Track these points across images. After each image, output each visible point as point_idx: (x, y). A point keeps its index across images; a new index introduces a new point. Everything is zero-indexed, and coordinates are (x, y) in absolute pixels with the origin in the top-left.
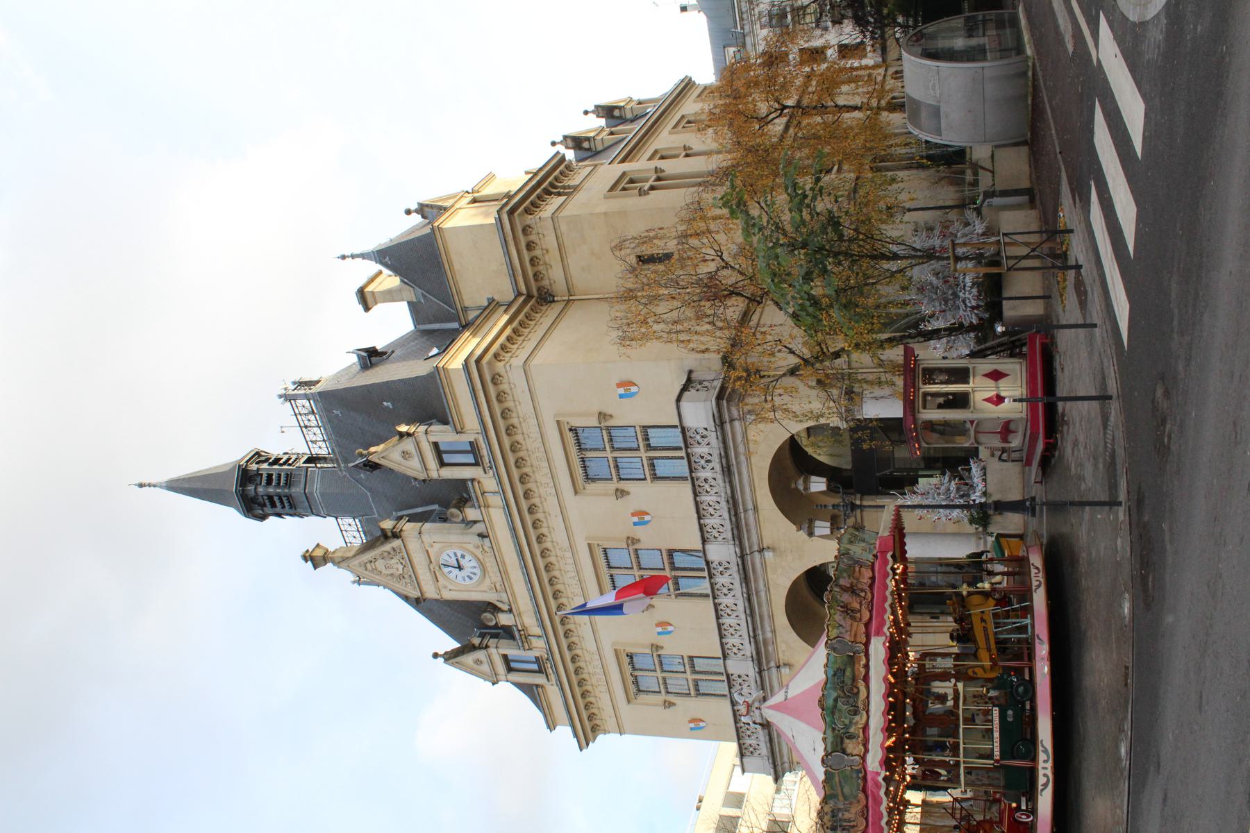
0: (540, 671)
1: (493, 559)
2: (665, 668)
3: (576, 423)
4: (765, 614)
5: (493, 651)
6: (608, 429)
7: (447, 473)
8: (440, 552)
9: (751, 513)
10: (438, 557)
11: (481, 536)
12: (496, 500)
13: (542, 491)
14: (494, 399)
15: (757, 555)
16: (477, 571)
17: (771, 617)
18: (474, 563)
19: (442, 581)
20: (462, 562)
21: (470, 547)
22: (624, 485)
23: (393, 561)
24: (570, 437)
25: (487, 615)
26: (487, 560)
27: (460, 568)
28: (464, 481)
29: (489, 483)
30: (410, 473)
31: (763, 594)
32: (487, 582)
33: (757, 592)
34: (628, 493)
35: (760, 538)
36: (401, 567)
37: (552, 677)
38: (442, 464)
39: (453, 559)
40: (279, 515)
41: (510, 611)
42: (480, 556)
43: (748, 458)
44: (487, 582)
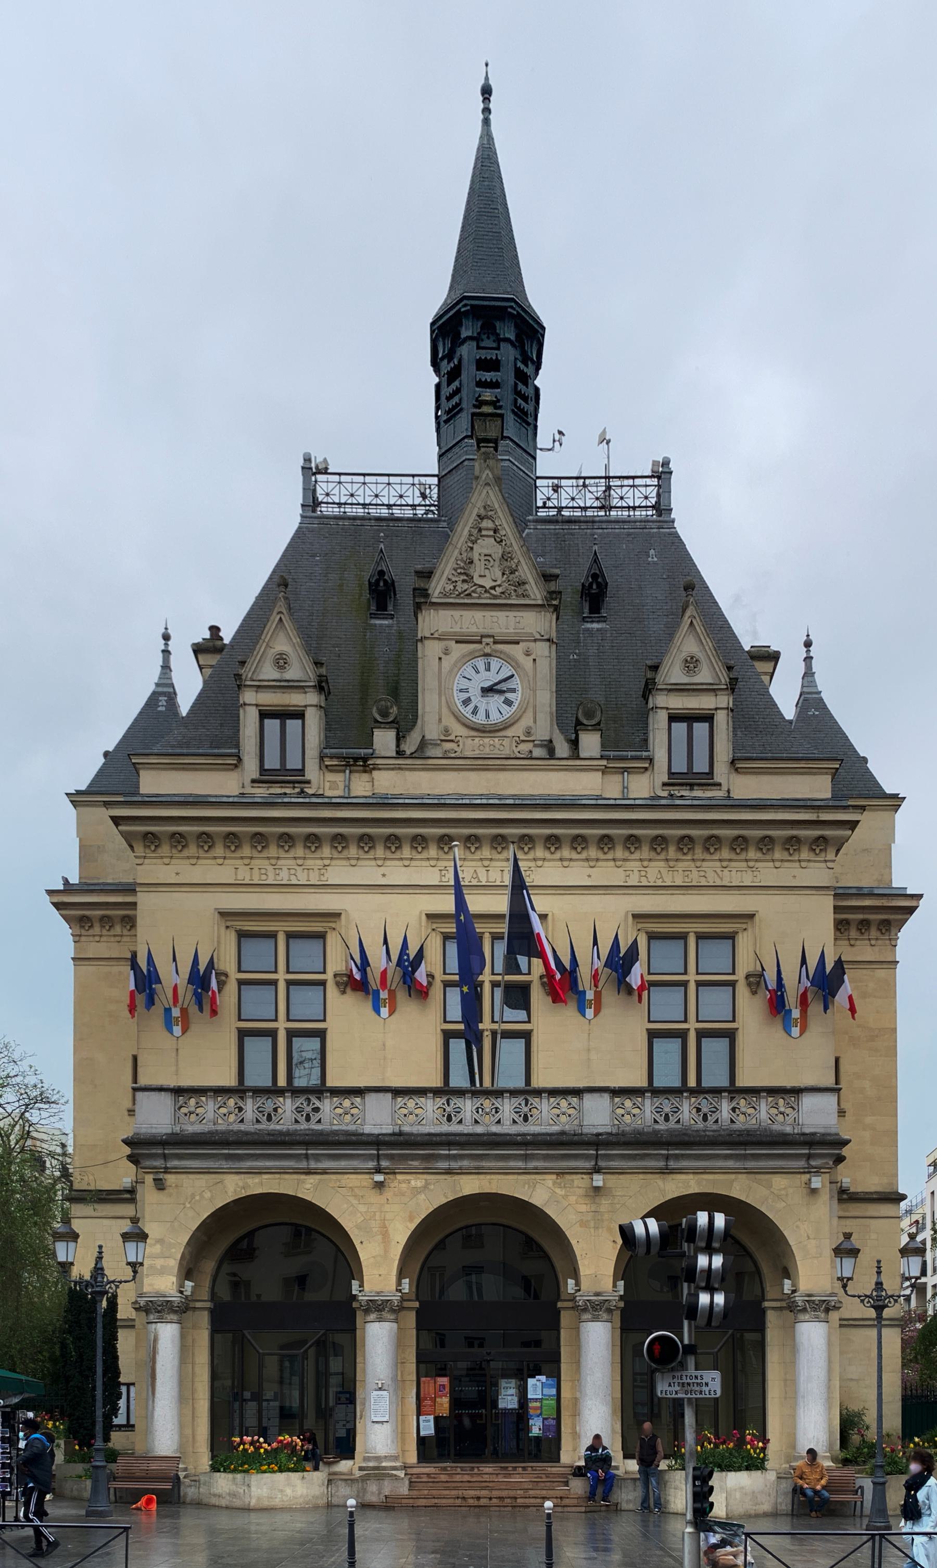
0: (263, 770)
1: (506, 752)
4: (484, 1164)
9: (662, 1164)
11: (549, 747)
12: (611, 788)
15: (589, 1164)
16: (480, 719)
17: (478, 1171)
18: (495, 718)
20: (497, 699)
21: (526, 721)
26: (506, 742)
28: (644, 743)
29: (641, 787)
31: (520, 1164)
33: (526, 1158)
35: (622, 1172)
37: (261, 792)
41: (400, 754)
42: (509, 732)
43: (749, 1172)
44: (458, 730)
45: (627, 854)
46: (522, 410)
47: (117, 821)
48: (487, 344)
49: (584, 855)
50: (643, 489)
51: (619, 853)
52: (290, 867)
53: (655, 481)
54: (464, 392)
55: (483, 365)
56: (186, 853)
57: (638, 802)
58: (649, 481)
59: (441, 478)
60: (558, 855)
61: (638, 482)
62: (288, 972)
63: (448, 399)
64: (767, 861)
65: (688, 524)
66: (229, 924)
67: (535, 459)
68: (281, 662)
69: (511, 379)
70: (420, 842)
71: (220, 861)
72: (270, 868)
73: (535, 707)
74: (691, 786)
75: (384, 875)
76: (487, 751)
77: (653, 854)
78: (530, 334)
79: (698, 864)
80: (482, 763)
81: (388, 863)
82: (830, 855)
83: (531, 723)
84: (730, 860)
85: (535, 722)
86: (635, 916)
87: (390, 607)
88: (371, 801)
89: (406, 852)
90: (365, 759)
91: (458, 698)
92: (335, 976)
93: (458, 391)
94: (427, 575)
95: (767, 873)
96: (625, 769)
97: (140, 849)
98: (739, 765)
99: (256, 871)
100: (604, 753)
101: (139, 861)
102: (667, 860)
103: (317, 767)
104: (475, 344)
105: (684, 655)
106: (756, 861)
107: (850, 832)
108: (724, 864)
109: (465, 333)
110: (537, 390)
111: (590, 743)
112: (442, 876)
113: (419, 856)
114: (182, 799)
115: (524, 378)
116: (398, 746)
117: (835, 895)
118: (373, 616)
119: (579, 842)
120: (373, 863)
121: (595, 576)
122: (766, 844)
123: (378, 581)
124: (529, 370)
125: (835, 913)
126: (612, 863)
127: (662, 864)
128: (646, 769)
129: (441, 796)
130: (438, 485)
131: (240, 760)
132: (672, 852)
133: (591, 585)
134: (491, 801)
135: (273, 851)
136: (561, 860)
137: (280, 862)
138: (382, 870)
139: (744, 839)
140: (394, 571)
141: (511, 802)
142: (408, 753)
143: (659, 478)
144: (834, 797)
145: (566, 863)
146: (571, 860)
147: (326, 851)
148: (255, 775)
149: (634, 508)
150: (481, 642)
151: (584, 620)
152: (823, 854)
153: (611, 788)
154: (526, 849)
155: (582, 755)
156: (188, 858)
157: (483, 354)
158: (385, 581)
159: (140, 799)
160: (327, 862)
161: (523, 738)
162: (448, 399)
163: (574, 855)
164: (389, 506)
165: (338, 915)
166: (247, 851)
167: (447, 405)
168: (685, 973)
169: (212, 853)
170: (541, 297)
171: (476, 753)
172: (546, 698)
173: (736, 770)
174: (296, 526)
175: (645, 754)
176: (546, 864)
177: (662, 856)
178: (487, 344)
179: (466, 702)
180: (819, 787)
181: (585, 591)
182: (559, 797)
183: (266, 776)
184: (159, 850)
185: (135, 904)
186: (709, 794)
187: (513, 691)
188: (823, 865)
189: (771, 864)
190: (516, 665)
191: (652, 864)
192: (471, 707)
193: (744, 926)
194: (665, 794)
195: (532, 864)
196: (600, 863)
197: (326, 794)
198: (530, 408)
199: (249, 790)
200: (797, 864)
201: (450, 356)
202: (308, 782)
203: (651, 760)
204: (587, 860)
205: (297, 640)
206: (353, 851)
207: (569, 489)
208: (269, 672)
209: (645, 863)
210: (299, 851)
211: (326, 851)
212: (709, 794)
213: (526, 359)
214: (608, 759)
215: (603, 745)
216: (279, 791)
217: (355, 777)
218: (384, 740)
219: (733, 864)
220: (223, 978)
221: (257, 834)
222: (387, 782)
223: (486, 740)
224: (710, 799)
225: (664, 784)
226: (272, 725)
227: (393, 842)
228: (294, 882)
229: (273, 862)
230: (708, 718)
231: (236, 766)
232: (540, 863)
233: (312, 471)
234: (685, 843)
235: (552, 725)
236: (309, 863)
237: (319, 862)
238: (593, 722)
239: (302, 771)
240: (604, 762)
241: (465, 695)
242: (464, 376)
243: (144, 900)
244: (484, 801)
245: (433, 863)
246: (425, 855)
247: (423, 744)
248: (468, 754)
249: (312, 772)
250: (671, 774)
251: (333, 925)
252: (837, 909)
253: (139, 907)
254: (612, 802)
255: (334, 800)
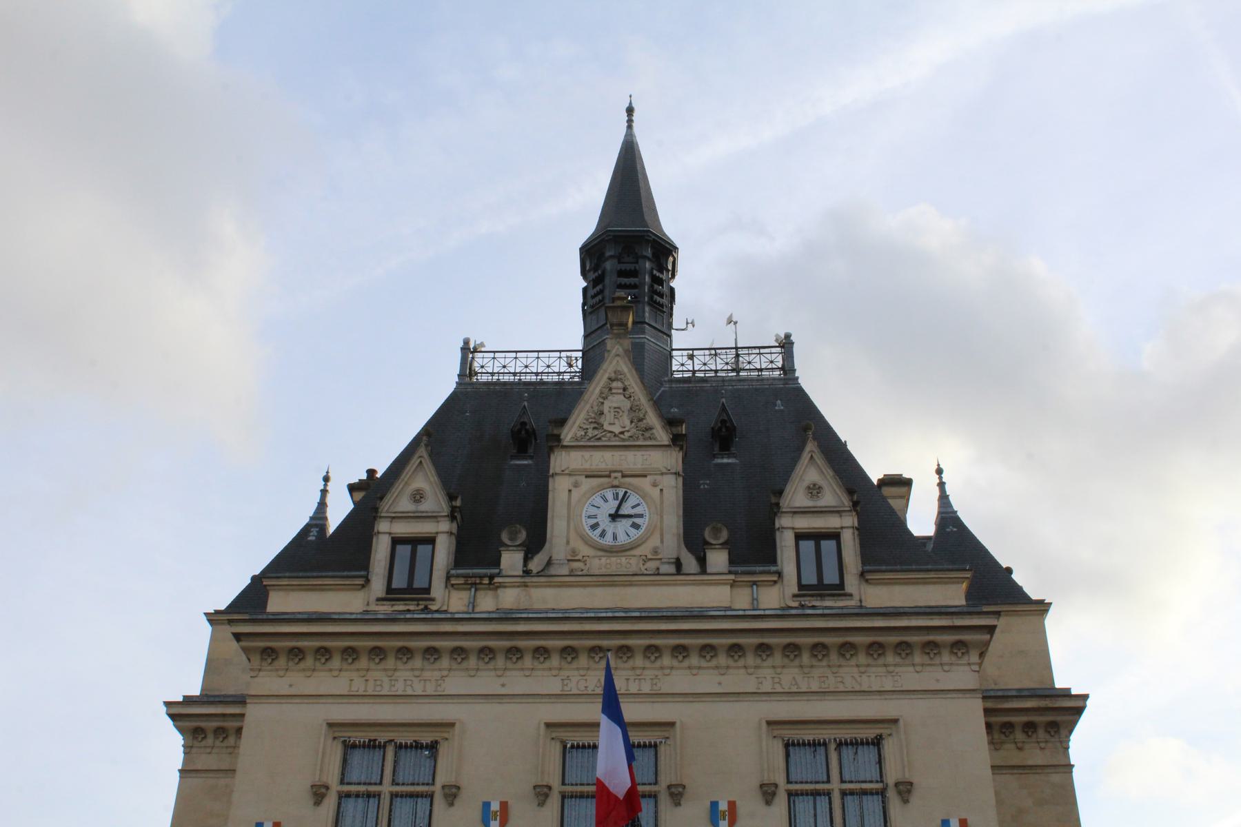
0: (389, 590)
1: (634, 569)
2: (350, 805)
3: (889, 747)
5: (445, 526)
6: (882, 793)
7: (786, 542)
8: (644, 496)
10: (637, 490)
11: (678, 564)
12: (741, 600)
13: (767, 673)
14: (931, 638)
18: (622, 539)
19: (587, 484)
20: (626, 523)
22: (554, 802)
23: (627, 422)
24: (869, 733)
25: (523, 536)
26: (633, 561)
27: (615, 517)
28: (773, 561)
29: (771, 598)
30: (789, 489)
32: (585, 550)
34: (541, 804)
36: (617, 429)
37: (385, 608)
38: (800, 537)
39: (424, 507)
40: (585, 290)
41: (527, 573)
44: (585, 550)
45: (759, 661)
46: (659, 304)
47: (238, 637)
48: (628, 261)
49: (714, 663)
50: (768, 356)
51: (750, 660)
52: (404, 677)
53: (779, 350)
54: (607, 292)
55: (621, 274)
56: (302, 665)
57: (767, 612)
58: (773, 350)
59: (584, 352)
60: (686, 663)
61: (762, 351)
62: (394, 783)
63: (593, 297)
64: (908, 665)
65: (810, 380)
66: (337, 734)
67: (670, 336)
68: (418, 497)
69: (647, 278)
70: (542, 653)
71: (336, 673)
72: (386, 679)
73: (662, 530)
74: (822, 596)
75: (503, 685)
76: (613, 569)
77: (786, 661)
78: (664, 251)
79: (835, 670)
80: (609, 580)
81: (508, 673)
82: (974, 658)
83: (658, 543)
84: (868, 665)
85: (662, 542)
86: (769, 723)
87: (531, 451)
88: (494, 616)
89: (528, 661)
90: (491, 577)
91: (586, 523)
92: (443, 787)
93: (601, 292)
94: (562, 422)
95: (911, 676)
96: (755, 583)
97: (256, 660)
98: (869, 577)
99: (371, 683)
100: (733, 569)
101: (253, 674)
102: (801, 667)
103: (443, 585)
104: (616, 261)
105: (806, 484)
106: (895, 665)
107: (988, 637)
108: (862, 669)
109: (608, 254)
110: (672, 290)
111: (718, 559)
112: (563, 685)
113: (541, 666)
114: (305, 616)
115: (660, 282)
116: (525, 564)
117: (984, 698)
118: (513, 457)
119: (708, 651)
120: (493, 673)
121: (723, 422)
122: (903, 649)
123: (519, 431)
124: (664, 277)
125: (985, 716)
126: (742, 671)
127: (796, 670)
128: (775, 582)
129: (566, 611)
130: (583, 358)
131: (368, 581)
132: (806, 658)
133: (720, 429)
134: (617, 614)
135: (391, 662)
136: (689, 668)
137: (397, 674)
138: (502, 680)
139: (881, 645)
140: (533, 423)
141: (637, 614)
142: (535, 571)
143: (782, 347)
144: (968, 606)
145: (694, 671)
146: (700, 668)
147: (445, 662)
148: (381, 594)
149: (761, 370)
150: (609, 476)
151: (714, 456)
152: (966, 658)
153: (741, 600)
154: (653, 658)
155: (709, 571)
156: (304, 670)
157: (623, 267)
158: (527, 431)
159: (265, 617)
160: (445, 673)
161: (650, 556)
162: (593, 297)
163: (704, 663)
164: (537, 374)
165: (452, 725)
166: (363, 662)
167: (591, 302)
168: (828, 781)
169: (329, 665)
170: (672, 220)
171: (603, 571)
172: (673, 522)
173: (867, 581)
174: (452, 390)
175: (773, 569)
176: (674, 672)
177: (797, 662)
178: (628, 261)
179: (594, 527)
180: (953, 594)
181: (715, 433)
182: (687, 609)
183: (392, 594)
184: (276, 663)
185: (243, 715)
186: (840, 604)
187: (641, 516)
188: (967, 668)
189: (911, 669)
190: (644, 496)
191: (785, 671)
192: (599, 531)
193: (888, 731)
194: (796, 604)
195: (659, 673)
196: (731, 671)
197: (451, 610)
198: (665, 301)
199: (373, 607)
200: (939, 668)
201: (595, 269)
202: (433, 600)
203: (780, 574)
204: (717, 667)
205: (434, 478)
206: (473, 661)
207: (700, 357)
208: (405, 505)
209: (779, 670)
210: (418, 662)
211: (445, 662)
212: (840, 604)
213: (662, 268)
214: (736, 573)
215: (732, 562)
216: (402, 608)
217: (481, 594)
218: (511, 560)
219: (874, 669)
220: (323, 790)
221: (375, 648)
222: (509, 598)
223: (614, 559)
224: (842, 608)
225: (795, 596)
226: (404, 551)
227: (514, 653)
228: (410, 692)
229: (390, 673)
230: (835, 536)
231: (363, 586)
232: (667, 671)
233: (468, 351)
234: (819, 650)
235: (679, 546)
236: (427, 674)
237: (437, 674)
238: (721, 541)
239: (427, 590)
240: (732, 577)
241: (593, 521)
242: (607, 281)
243: (253, 712)
244: (610, 615)
245: (554, 672)
246: (547, 664)
247: (549, 563)
248: (597, 572)
249: (438, 590)
250: (801, 586)
251: (446, 735)
252: (987, 711)
253: (247, 718)
254: (741, 613)
255: (457, 616)
